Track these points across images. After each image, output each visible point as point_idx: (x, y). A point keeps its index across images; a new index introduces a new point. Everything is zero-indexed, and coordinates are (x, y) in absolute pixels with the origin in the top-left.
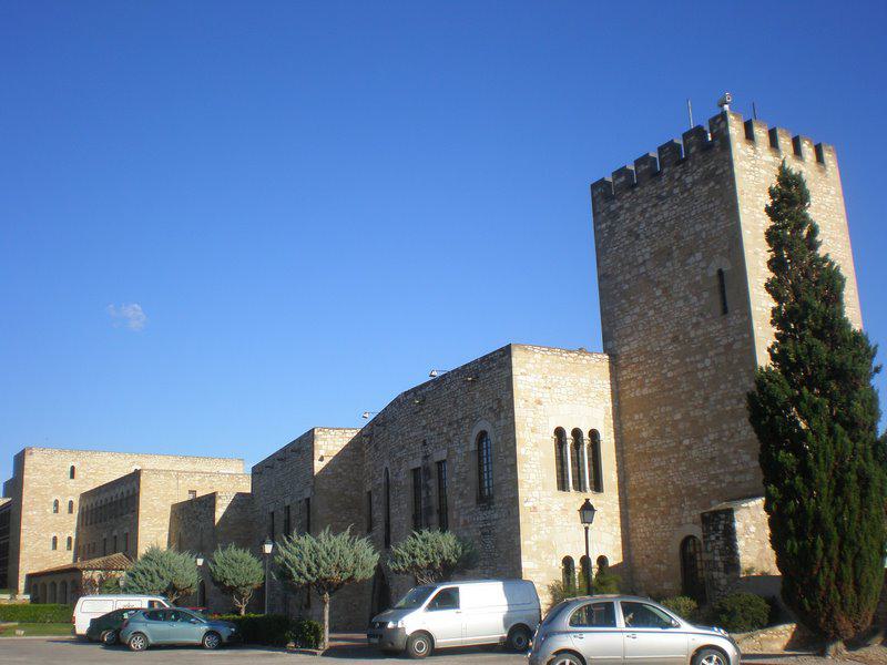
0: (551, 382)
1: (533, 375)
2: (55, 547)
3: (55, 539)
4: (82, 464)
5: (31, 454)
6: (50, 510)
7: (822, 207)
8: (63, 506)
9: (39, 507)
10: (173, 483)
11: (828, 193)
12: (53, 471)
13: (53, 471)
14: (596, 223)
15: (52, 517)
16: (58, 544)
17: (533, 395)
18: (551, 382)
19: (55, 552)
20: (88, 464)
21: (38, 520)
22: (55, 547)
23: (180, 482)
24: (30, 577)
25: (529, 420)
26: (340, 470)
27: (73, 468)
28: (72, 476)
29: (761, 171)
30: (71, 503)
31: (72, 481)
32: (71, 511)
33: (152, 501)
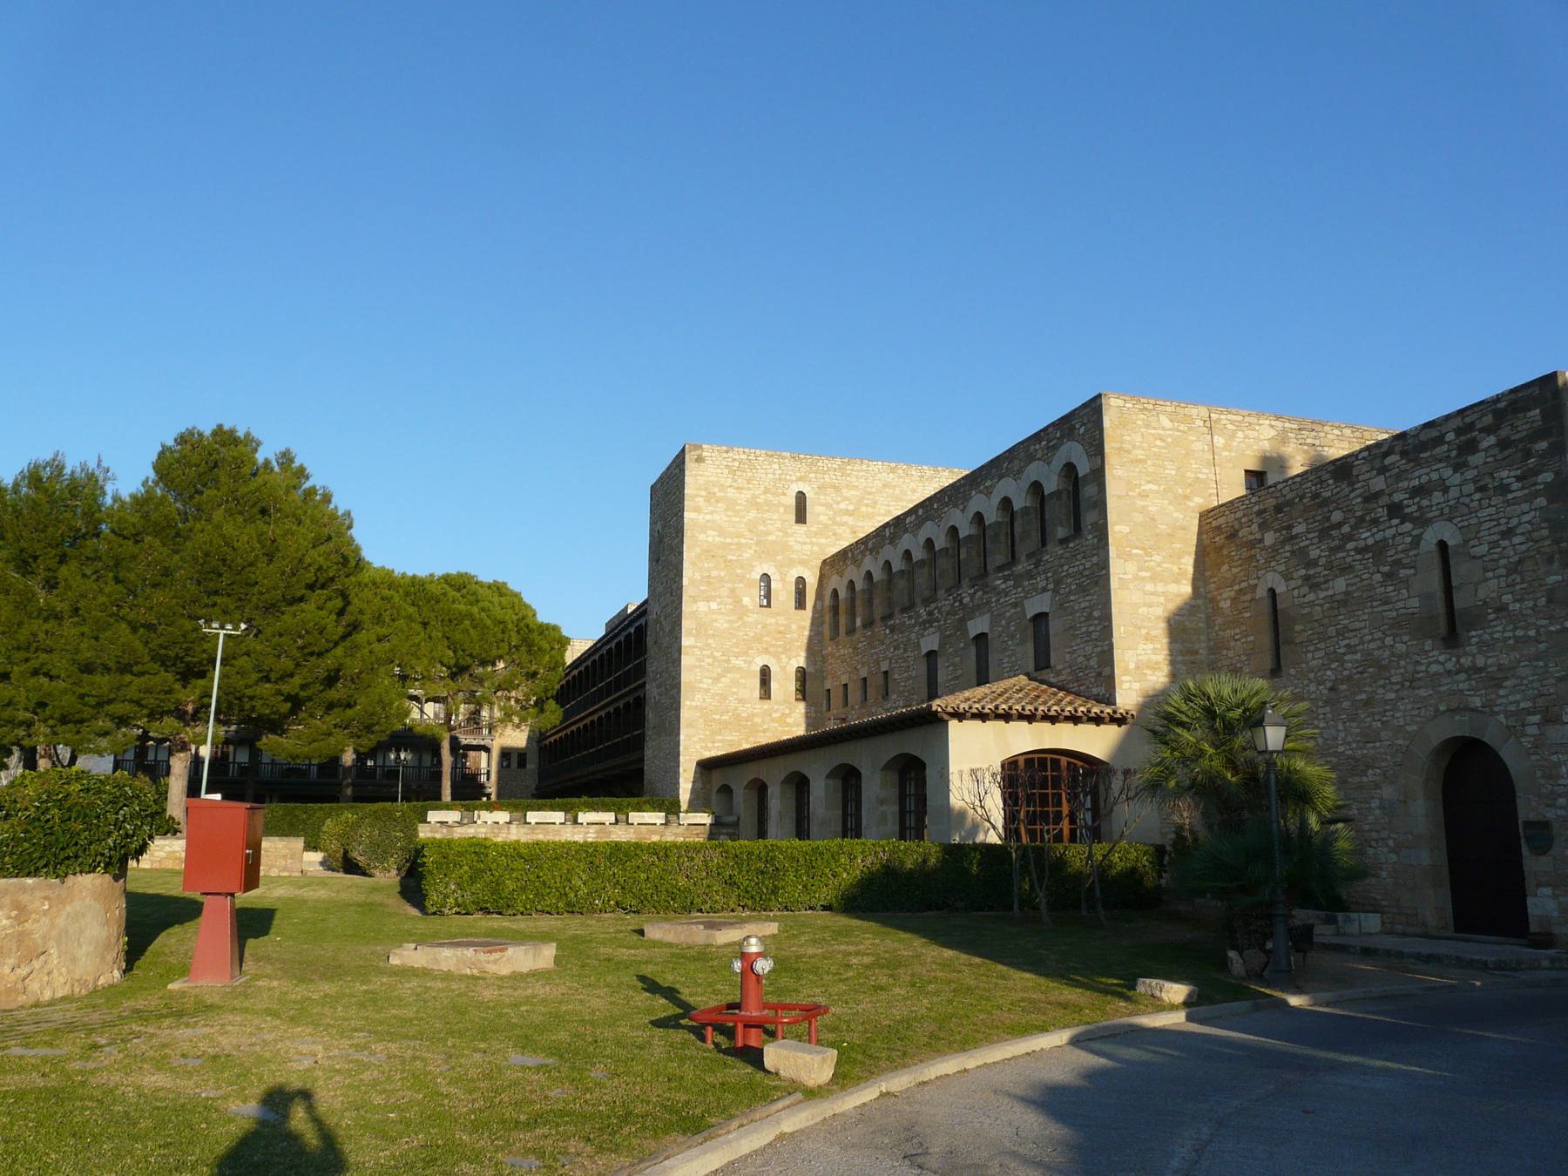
2: (766, 693)
4: (822, 488)
5: (700, 459)
6: (751, 598)
8: (783, 593)
9: (724, 592)
10: (1200, 446)
12: (753, 503)
13: (753, 503)
15: (756, 617)
16: (774, 685)
19: (766, 705)
20: (837, 489)
21: (722, 624)
22: (766, 693)
23: (1219, 441)
24: (707, 767)
27: (801, 499)
28: (801, 517)
30: (801, 581)
31: (801, 528)
32: (800, 603)
33: (1144, 495)
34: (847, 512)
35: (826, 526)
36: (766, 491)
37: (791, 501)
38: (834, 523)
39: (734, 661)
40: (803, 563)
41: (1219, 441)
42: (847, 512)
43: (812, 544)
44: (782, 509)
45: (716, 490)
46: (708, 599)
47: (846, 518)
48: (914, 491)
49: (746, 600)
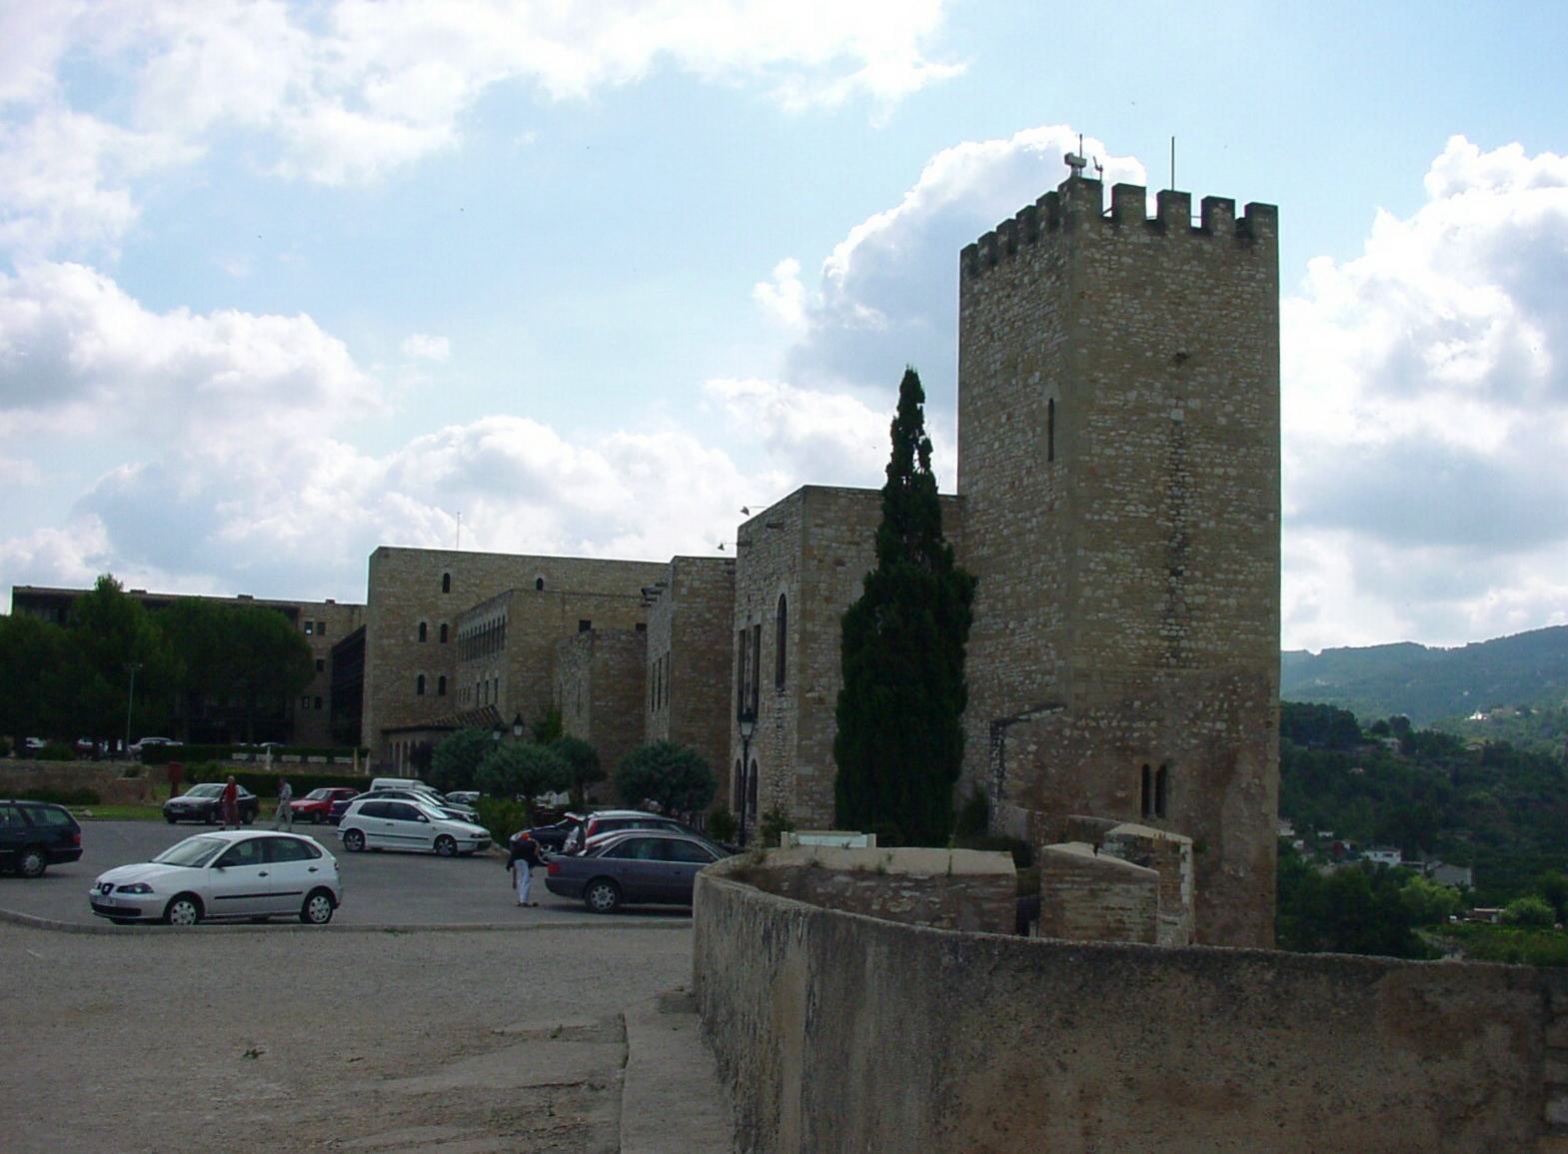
0: (861, 535)
1: (834, 526)
2: (421, 691)
3: (421, 678)
6: (413, 637)
7: (1234, 301)
10: (557, 611)
11: (1252, 278)
14: (962, 310)
16: (426, 687)
17: (831, 553)
18: (861, 535)
22: (421, 691)
23: (568, 607)
25: (823, 586)
26: (708, 616)
27: (447, 576)
28: (446, 589)
29: (1126, 260)
31: (446, 595)
34: (476, 586)
35: (462, 593)
36: (427, 573)
37: (440, 579)
38: (467, 592)
39: (407, 674)
40: (445, 615)
41: (568, 607)
42: (476, 586)
43: (452, 604)
44: (435, 584)
45: (395, 573)
46: (387, 637)
47: (474, 588)
48: (518, 571)
49: (411, 638)
